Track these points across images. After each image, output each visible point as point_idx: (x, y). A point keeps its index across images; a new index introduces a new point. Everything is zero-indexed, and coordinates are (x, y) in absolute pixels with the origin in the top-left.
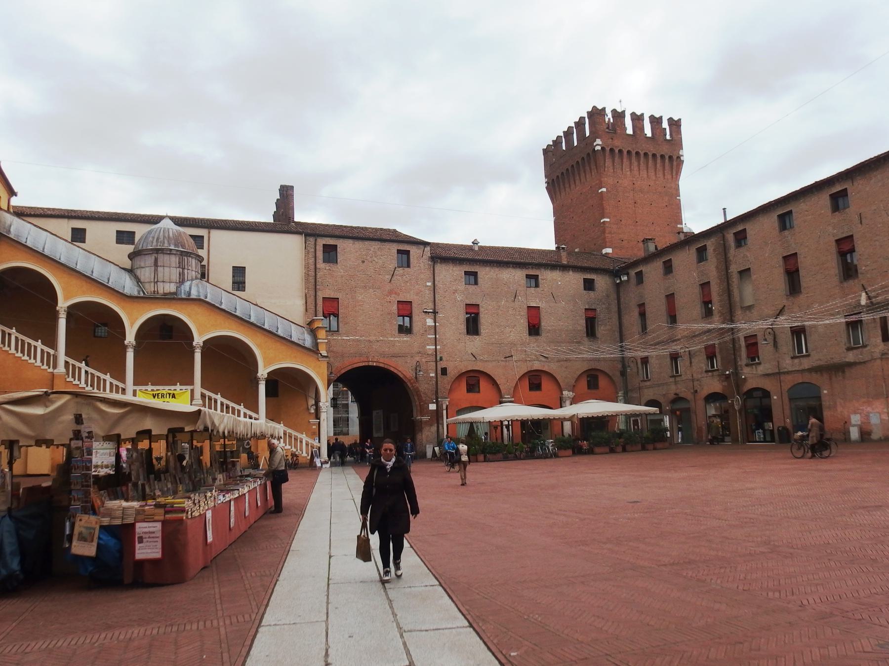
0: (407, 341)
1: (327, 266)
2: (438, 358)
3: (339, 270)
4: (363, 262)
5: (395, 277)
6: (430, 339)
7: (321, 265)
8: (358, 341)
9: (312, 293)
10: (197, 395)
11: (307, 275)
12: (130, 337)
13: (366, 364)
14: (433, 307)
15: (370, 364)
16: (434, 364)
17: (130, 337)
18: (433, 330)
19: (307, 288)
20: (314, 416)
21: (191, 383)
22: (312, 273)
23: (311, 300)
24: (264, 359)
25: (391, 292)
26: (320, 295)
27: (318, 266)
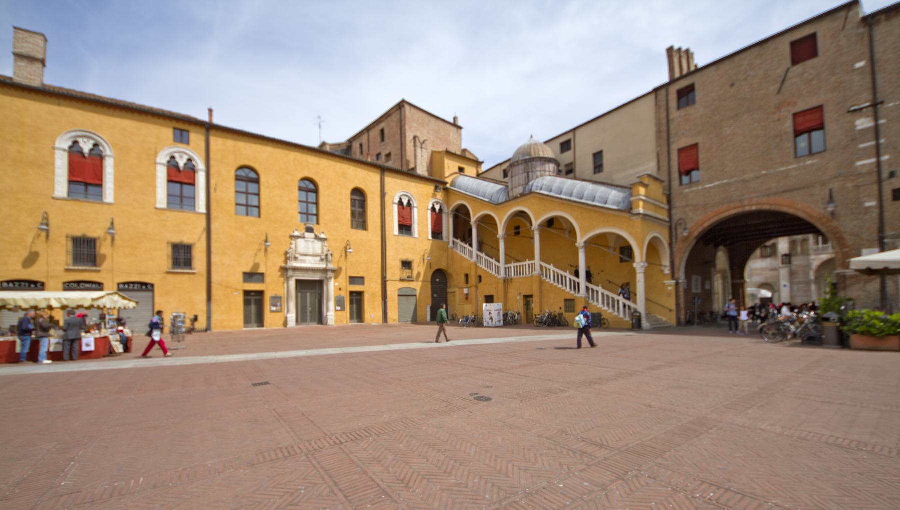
0: (812, 165)
1: (683, 112)
2: (885, 174)
3: (697, 110)
4: (732, 85)
5: (787, 83)
6: (865, 149)
7: (675, 113)
9: (665, 149)
10: (538, 267)
11: (659, 132)
12: (501, 232)
13: (740, 210)
14: (871, 97)
15: (747, 208)
16: (875, 187)
17: (501, 232)
18: (872, 134)
19: (659, 145)
20: (670, 276)
21: (532, 258)
22: (664, 128)
23: (664, 158)
24: (581, 229)
25: (779, 107)
26: (675, 148)
27: (671, 117)
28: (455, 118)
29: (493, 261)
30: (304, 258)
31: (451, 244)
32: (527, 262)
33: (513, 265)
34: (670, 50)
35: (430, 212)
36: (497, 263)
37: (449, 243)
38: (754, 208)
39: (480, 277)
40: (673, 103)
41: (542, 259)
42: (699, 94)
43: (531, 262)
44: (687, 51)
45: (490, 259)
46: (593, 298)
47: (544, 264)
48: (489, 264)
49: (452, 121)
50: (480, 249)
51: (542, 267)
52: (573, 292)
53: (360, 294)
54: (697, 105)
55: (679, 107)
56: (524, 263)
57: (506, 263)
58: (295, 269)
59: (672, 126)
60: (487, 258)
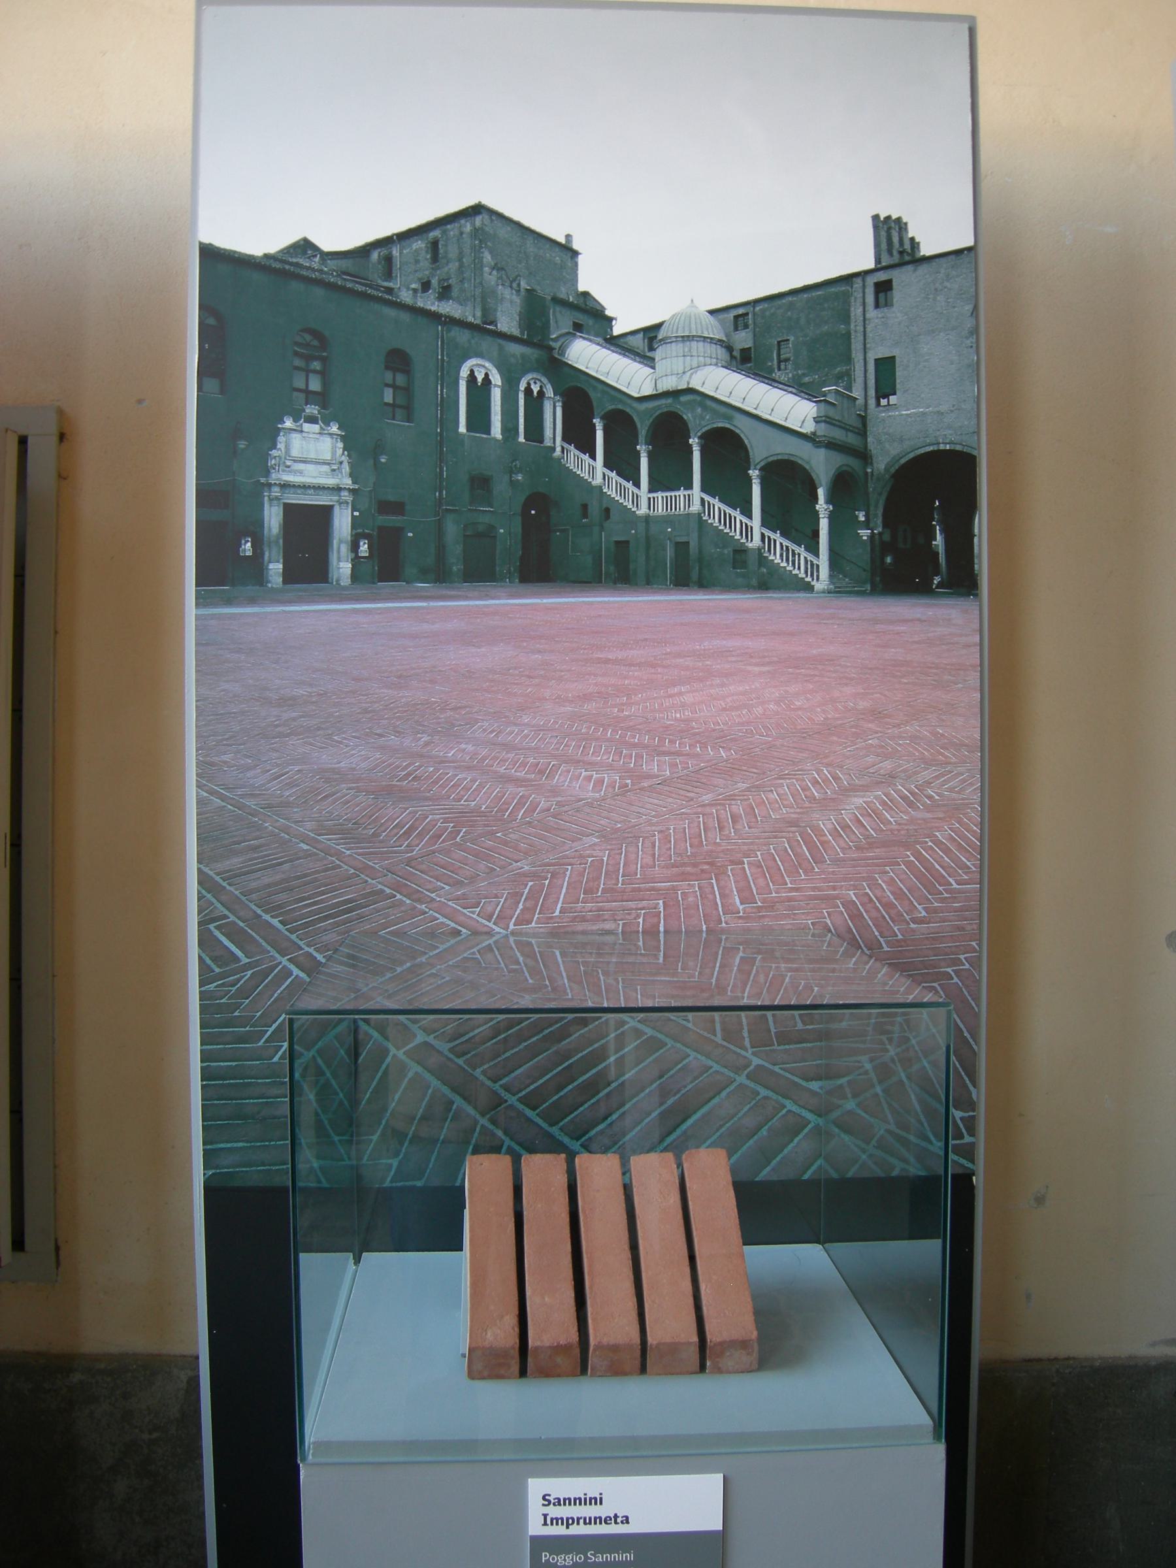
3: (897, 313)
7: (872, 313)
8: (923, 414)
13: (935, 448)
15: (942, 447)
21: (689, 486)
27: (868, 316)
28: (568, 237)
29: (629, 485)
30: (301, 466)
31: (558, 449)
32: (682, 493)
33: (660, 495)
34: (876, 218)
35: (521, 396)
36: (636, 490)
37: (554, 449)
38: (948, 447)
39: (607, 510)
40: (870, 299)
41: (703, 490)
42: (897, 294)
43: (686, 493)
44: (899, 220)
45: (624, 483)
46: (769, 550)
47: (707, 498)
48: (622, 491)
49: (562, 240)
50: (608, 464)
51: (703, 500)
52: (744, 540)
53: (398, 532)
54: (894, 309)
55: (877, 306)
56: (677, 494)
57: (650, 491)
58: (285, 486)
59: (869, 329)
60: (620, 480)
